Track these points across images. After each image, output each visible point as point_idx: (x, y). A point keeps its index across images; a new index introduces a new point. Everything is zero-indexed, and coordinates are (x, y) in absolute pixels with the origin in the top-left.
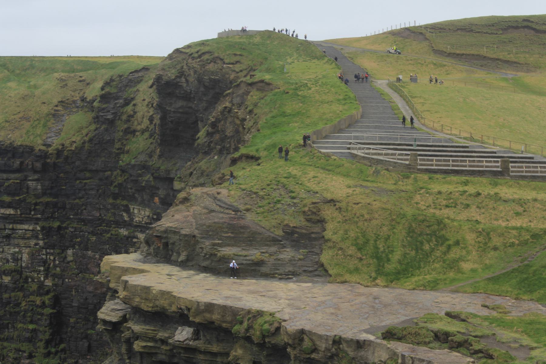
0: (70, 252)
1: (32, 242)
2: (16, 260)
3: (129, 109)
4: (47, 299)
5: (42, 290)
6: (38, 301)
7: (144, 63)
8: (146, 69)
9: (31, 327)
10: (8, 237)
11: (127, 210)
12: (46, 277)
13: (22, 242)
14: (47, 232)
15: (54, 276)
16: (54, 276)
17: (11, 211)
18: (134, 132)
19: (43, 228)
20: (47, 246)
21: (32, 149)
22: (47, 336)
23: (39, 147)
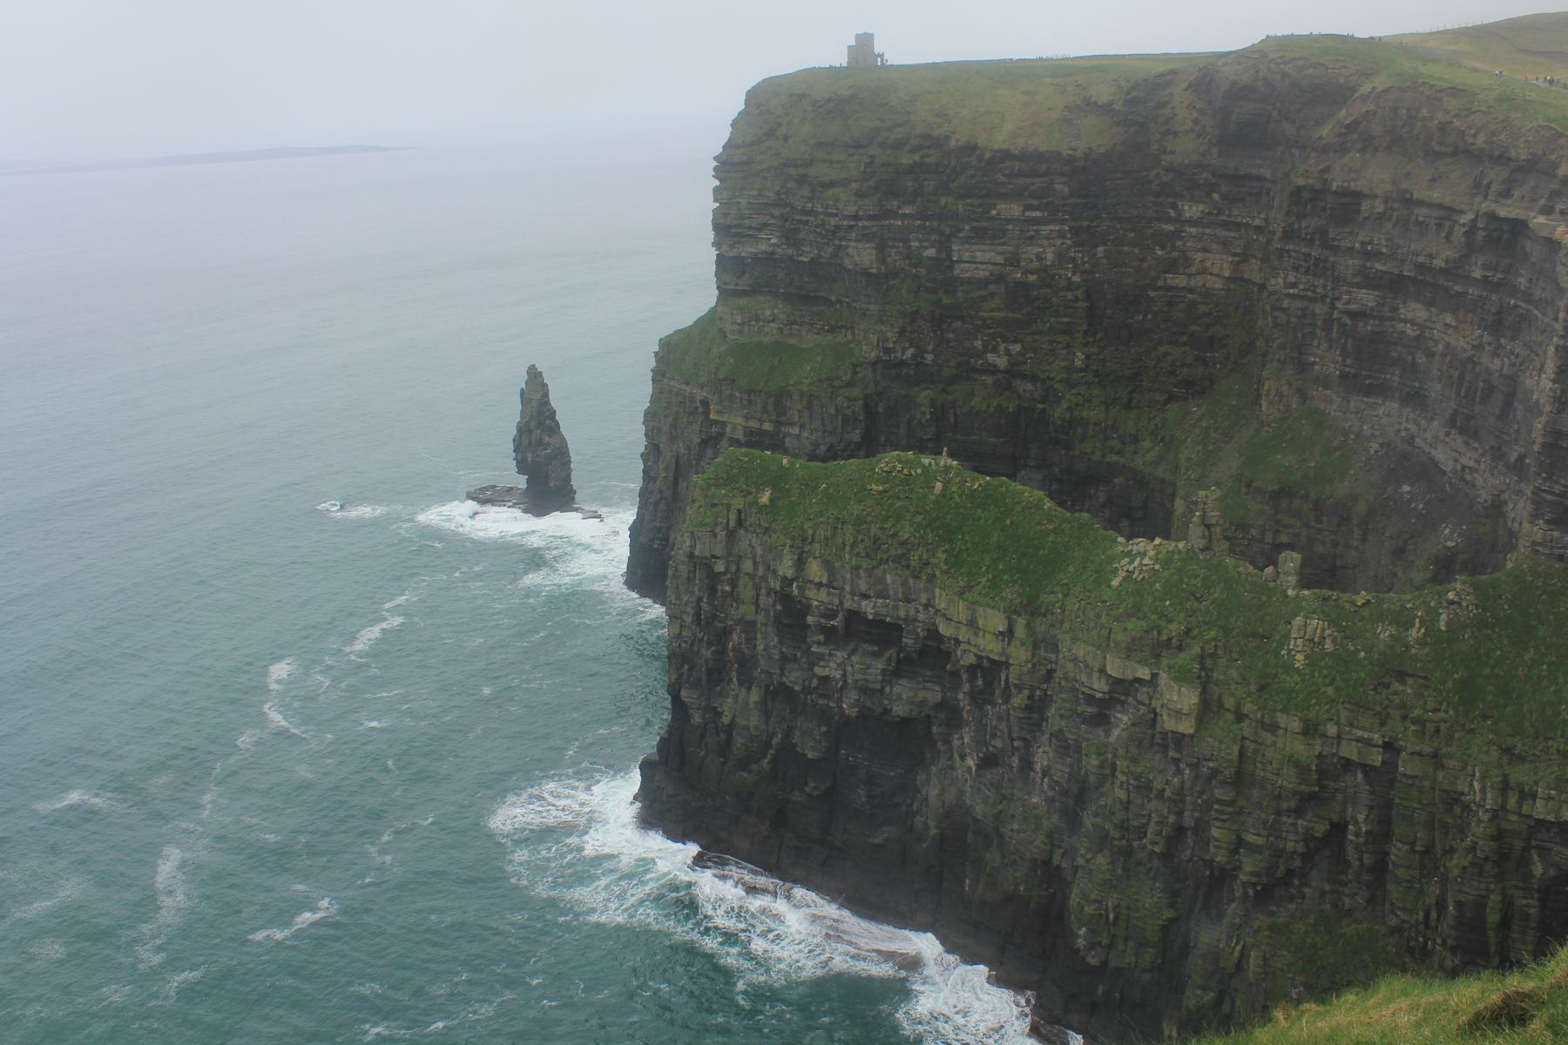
0: (1101, 249)
1: (1059, 242)
2: (1040, 258)
3: (1167, 111)
4: (1079, 293)
5: (1070, 286)
6: (1070, 296)
7: (1161, 68)
8: (1173, 72)
9: (1066, 320)
10: (1031, 238)
11: (1174, 206)
12: (1074, 273)
13: (1046, 242)
14: (1076, 231)
15: (1083, 272)
16: (1083, 272)
17: (1038, 214)
18: (1175, 134)
19: (1071, 228)
20: (1076, 245)
21: (1059, 154)
22: (1085, 327)
23: (1066, 152)
